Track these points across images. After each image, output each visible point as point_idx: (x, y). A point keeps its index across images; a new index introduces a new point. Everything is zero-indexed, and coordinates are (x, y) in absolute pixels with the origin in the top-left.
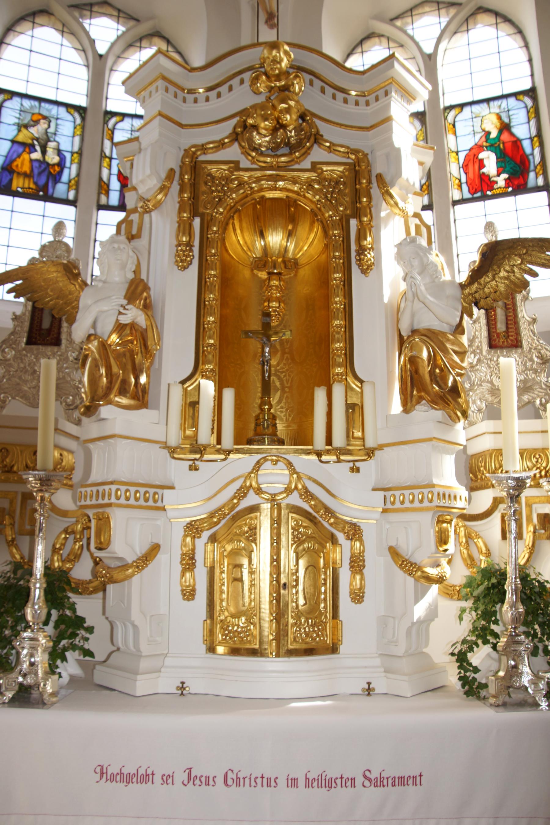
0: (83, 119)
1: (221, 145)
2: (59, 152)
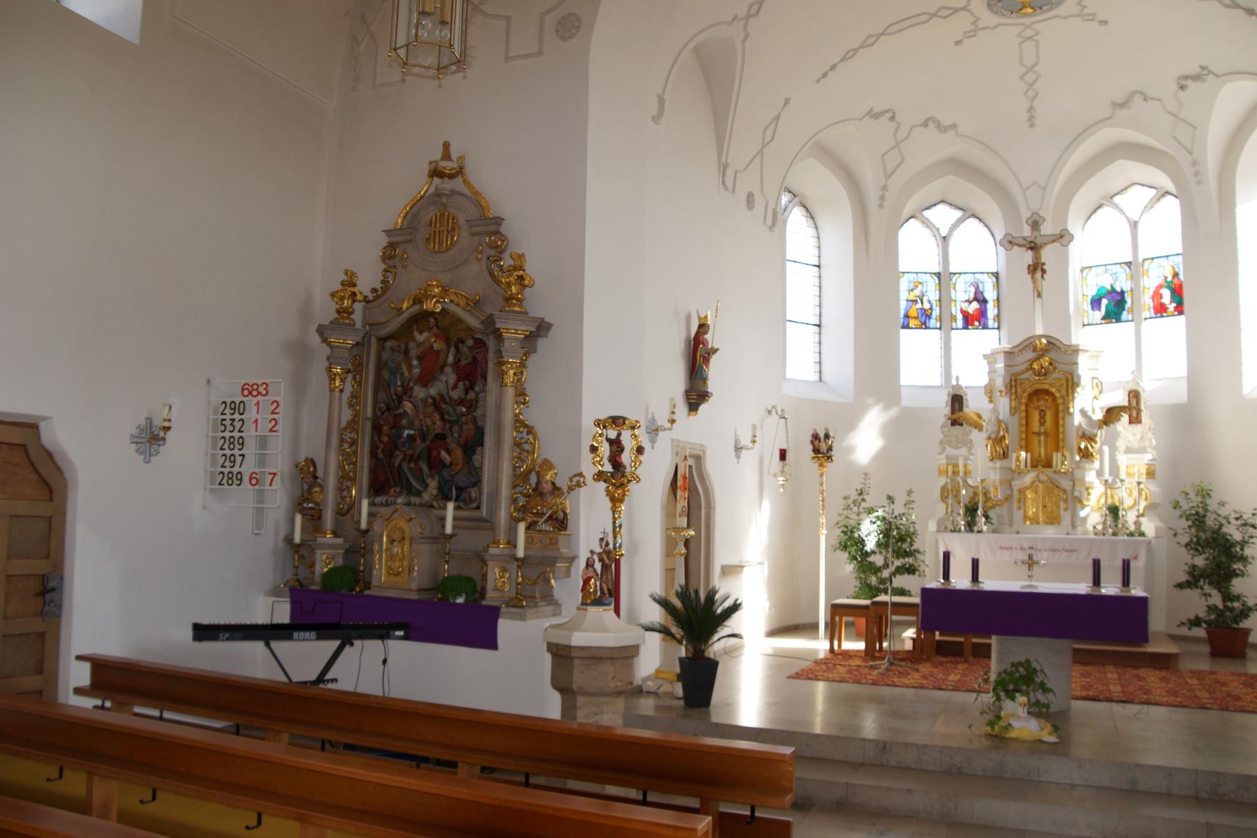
1: (1023, 372)
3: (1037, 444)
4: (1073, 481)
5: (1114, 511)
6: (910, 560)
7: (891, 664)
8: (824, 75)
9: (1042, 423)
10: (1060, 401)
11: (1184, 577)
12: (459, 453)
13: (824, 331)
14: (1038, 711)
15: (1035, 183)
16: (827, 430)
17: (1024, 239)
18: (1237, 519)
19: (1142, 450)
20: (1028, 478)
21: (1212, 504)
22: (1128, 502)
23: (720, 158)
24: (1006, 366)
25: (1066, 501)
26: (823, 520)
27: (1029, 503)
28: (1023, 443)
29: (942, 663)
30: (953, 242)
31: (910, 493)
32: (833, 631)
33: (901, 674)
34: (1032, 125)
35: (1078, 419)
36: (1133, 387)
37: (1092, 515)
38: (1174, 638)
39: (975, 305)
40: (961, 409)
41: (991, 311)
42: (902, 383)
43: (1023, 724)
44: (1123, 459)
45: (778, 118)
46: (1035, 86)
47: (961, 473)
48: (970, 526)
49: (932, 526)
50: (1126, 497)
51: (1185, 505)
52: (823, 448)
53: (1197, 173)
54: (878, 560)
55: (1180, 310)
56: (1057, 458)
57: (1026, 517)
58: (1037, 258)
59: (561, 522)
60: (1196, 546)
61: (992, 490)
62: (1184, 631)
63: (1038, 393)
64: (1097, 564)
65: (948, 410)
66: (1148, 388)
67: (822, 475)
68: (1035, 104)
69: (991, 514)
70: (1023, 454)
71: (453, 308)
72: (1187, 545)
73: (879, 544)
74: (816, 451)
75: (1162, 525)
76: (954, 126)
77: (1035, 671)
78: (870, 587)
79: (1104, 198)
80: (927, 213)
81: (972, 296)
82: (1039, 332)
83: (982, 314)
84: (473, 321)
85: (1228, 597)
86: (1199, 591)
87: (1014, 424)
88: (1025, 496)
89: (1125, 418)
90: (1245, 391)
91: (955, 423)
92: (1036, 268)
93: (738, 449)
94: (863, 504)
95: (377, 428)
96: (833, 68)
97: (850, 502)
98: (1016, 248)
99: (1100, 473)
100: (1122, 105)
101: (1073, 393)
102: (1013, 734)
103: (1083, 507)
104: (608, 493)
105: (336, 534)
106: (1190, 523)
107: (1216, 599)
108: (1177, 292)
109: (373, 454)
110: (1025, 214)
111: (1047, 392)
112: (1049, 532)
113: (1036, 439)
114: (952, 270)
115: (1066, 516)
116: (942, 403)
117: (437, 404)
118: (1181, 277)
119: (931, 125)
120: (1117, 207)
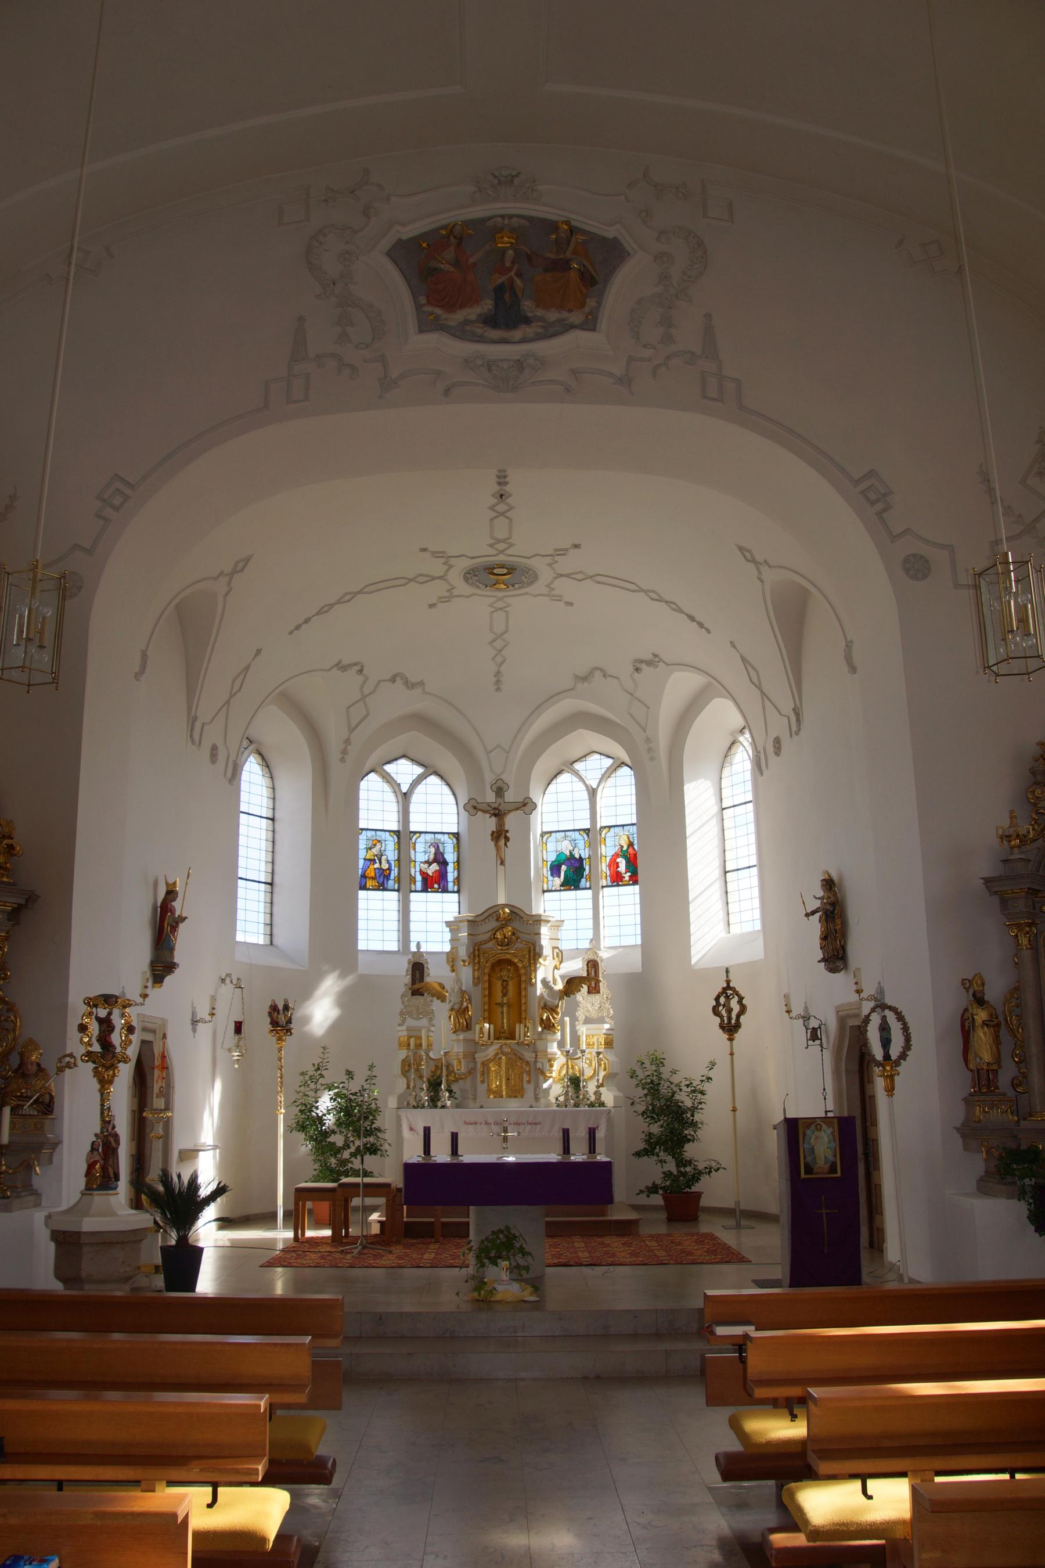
0: (399, 838)
1: (486, 942)
2: (388, 862)
3: (500, 1016)
4: (536, 1052)
5: (575, 1082)
6: (372, 1139)
7: (364, 1247)
8: (298, 628)
9: (505, 995)
10: (522, 971)
11: (642, 1146)
13: (276, 889)
14: (518, 1273)
15: (498, 746)
16: (286, 1001)
17: (489, 805)
18: (688, 1086)
19: (601, 1021)
20: (491, 1051)
21: (665, 1072)
22: (588, 1073)
23: (189, 709)
24: (469, 934)
25: (529, 1073)
26: (281, 1098)
27: (493, 1075)
28: (486, 1014)
29: (413, 1245)
30: (415, 798)
31: (371, 1067)
32: (295, 1218)
33: (376, 1257)
34: (498, 689)
35: (539, 989)
36: (591, 957)
37: (554, 1087)
38: (635, 1207)
39: (435, 867)
40: (422, 979)
41: (451, 875)
42: (362, 946)
43: (505, 1286)
44: (583, 1030)
45: (247, 668)
46: (503, 652)
47: (424, 1046)
48: (434, 1101)
49: (392, 1102)
50: (586, 1067)
51: (641, 1074)
52: (282, 1019)
53: (650, 750)
54: (338, 1140)
55: (634, 880)
56: (519, 1029)
57: (490, 1091)
58: (501, 825)
59: (47, 1106)
60: (651, 1114)
61: (455, 1063)
62: (643, 1200)
63: (501, 964)
64: (566, 1133)
65: (408, 979)
66: (604, 954)
67: (280, 1050)
68: (502, 669)
69: (455, 1087)
70: (487, 1025)
72: (643, 1113)
73: (339, 1123)
74: (274, 1023)
75: (621, 1094)
76: (421, 684)
77: (515, 1237)
78: (332, 1170)
79: (564, 764)
80: (388, 768)
81: (432, 857)
82: (501, 900)
83: (442, 875)
85: (681, 1162)
86: (655, 1158)
88: (489, 1069)
89: (585, 989)
90: (694, 961)
91: (416, 993)
92: (500, 835)
93: (195, 1022)
94: (321, 1080)
96: (307, 621)
97: (307, 1077)
98: (479, 813)
99: (561, 1044)
100: (585, 679)
101: (535, 964)
102: (498, 1297)
103: (545, 1081)
104: (96, 1073)
106: (646, 1091)
107: (671, 1166)
108: (632, 862)
110: (489, 778)
111: (510, 962)
112: (513, 1105)
113: (499, 1010)
114: (412, 829)
115: (529, 1089)
116: (402, 969)
118: (636, 847)
120: (576, 773)
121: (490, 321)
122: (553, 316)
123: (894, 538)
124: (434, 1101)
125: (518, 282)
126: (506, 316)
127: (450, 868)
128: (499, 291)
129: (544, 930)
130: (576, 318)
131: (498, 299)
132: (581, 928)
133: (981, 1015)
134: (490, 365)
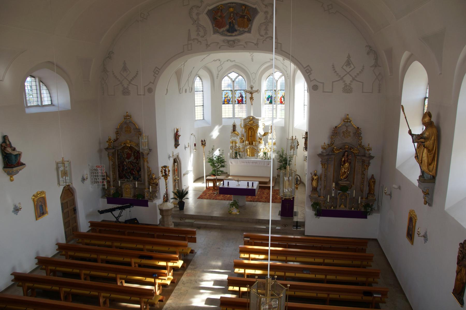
6: (223, 164)
12: (136, 172)
20: (248, 147)
26: (204, 159)
35: (258, 134)
39: (240, 98)
41: (244, 100)
48: (236, 157)
56: (254, 143)
58: (252, 96)
59: (157, 184)
60: (281, 161)
63: (250, 128)
71: (132, 146)
74: (202, 144)
76: (234, 61)
83: (242, 100)
84: (137, 148)
87: (245, 135)
92: (251, 98)
93: (185, 148)
95: (119, 167)
105: (114, 186)
109: (119, 171)
115: (256, 155)
117: (131, 163)
119: (229, 61)
121: (228, 31)
122: (241, 29)
123: (311, 81)
124: (236, 157)
125: (234, 21)
126: (232, 30)
127: (244, 98)
128: (230, 23)
129: (260, 122)
130: (246, 30)
131: (230, 25)
132: (269, 117)
133: (315, 178)
134: (228, 41)
